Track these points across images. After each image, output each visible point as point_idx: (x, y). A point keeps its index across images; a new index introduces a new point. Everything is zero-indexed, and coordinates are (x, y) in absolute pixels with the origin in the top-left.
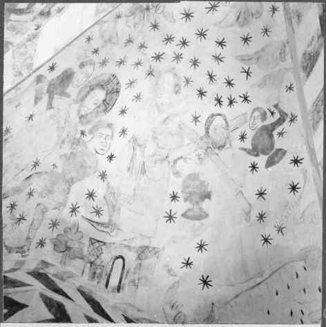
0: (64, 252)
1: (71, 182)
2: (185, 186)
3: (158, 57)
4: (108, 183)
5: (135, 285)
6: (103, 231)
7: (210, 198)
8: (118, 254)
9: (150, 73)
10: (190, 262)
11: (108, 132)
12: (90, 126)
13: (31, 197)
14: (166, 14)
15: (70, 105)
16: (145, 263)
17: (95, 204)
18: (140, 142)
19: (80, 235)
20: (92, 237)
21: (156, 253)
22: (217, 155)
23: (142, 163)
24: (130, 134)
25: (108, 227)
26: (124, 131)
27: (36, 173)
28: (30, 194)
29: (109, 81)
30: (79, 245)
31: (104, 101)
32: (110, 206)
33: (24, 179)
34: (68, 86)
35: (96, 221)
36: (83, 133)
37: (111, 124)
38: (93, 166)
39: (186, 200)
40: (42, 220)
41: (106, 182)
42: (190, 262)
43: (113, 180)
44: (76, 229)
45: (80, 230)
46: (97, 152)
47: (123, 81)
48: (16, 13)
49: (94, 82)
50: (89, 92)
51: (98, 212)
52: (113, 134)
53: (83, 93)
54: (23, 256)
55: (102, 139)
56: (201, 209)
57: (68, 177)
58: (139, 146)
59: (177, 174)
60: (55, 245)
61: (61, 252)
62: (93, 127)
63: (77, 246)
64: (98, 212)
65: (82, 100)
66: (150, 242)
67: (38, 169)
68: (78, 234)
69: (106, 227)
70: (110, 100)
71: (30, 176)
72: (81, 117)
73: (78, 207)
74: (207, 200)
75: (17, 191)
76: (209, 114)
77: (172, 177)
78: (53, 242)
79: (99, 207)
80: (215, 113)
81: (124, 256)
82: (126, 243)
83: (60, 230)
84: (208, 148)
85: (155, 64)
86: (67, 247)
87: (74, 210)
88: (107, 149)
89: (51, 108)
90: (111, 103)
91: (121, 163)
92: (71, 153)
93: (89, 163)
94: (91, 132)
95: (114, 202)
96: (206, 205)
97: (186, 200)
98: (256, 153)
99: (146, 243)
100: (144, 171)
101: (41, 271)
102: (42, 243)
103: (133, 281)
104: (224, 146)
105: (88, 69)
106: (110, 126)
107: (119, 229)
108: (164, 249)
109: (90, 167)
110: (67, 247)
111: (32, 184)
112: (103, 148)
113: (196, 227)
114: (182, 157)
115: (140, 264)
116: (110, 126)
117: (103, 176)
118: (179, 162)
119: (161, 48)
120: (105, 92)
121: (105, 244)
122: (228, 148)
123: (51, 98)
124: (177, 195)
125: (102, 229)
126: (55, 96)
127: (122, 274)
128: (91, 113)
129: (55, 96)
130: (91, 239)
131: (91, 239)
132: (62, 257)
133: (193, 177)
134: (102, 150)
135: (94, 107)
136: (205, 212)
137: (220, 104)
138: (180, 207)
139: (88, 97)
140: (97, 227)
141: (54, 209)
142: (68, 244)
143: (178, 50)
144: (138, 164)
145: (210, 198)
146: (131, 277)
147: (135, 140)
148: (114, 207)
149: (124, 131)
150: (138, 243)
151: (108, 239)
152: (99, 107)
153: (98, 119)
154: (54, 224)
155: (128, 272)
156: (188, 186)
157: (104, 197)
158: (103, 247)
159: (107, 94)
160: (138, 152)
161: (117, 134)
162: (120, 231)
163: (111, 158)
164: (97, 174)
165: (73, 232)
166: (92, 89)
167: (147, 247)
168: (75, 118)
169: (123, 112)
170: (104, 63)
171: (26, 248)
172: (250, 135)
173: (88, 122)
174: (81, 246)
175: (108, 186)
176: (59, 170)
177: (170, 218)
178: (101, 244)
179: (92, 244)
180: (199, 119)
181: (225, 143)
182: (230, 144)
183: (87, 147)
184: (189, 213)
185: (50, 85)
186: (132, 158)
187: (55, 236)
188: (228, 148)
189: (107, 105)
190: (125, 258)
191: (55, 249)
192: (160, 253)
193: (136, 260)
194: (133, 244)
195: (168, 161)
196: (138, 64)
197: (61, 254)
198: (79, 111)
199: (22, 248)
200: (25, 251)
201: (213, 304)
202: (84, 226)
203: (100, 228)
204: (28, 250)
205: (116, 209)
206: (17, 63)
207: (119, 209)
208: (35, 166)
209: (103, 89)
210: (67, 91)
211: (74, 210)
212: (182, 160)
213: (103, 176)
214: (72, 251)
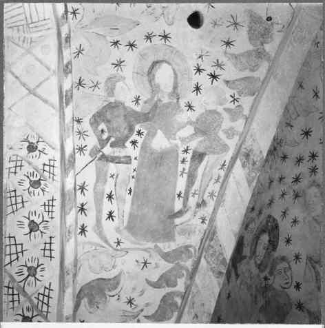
3: (297, 180)
4: (308, 310)
9: (297, 196)
11: (284, 265)
12: (268, 270)
14: (289, 142)
24: (304, 257)
31: (270, 241)
41: (305, 310)
47: (277, 215)
48: (178, 217)
52: (288, 264)
58: (316, 263)
85: (296, 187)
94: (271, 273)
116: (283, 259)
119: (297, 171)
134: (287, 283)
135: (264, 251)
143: (310, 165)
147: (310, 259)
149: (297, 257)
159: (269, 235)
160: (317, 266)
163: (298, 286)
168: (255, 271)
170: (260, 213)
173: (266, 267)
183: (274, 289)
186: (316, 277)
189: (273, 244)
196: (283, 194)
198: (256, 262)
206: (214, 265)
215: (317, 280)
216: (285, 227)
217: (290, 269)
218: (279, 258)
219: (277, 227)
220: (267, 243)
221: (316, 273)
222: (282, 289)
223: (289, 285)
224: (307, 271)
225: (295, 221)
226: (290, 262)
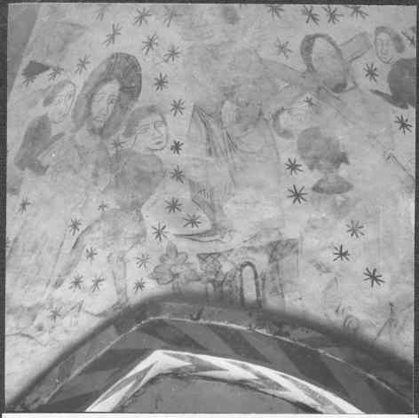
2: (303, 149)
4: (190, 181)
5: (278, 294)
7: (347, 162)
8: (242, 262)
10: (343, 251)
13: (95, 256)
16: (284, 262)
17: (183, 214)
21: (293, 246)
22: (338, 99)
25: (216, 234)
27: (83, 232)
31: (122, 89)
35: (195, 232)
37: (153, 106)
39: (311, 168)
42: (343, 251)
43: (195, 174)
56: (337, 177)
59: (286, 134)
60: (157, 279)
61: (169, 282)
62: (129, 126)
64: (193, 222)
66: (280, 234)
67: (82, 228)
68: (180, 257)
69: (213, 235)
71: (78, 239)
74: (343, 165)
76: (300, 37)
77: (280, 140)
78: (153, 278)
80: (312, 32)
81: (251, 261)
82: (247, 245)
84: (319, 88)
96: (343, 171)
97: (311, 168)
98: (401, 104)
99: (274, 237)
100: (233, 146)
103: (275, 289)
104: (344, 85)
106: (152, 110)
107: (230, 231)
108: (302, 239)
111: (85, 246)
112: (158, 140)
113: (339, 204)
114: (283, 109)
115: (277, 267)
116: (152, 110)
117: (178, 175)
118: (283, 118)
120: (115, 81)
121: (220, 254)
122: (352, 89)
124: (297, 163)
125: (213, 238)
126: (39, 158)
127: (257, 285)
128: (113, 113)
129: (39, 158)
130: (199, 256)
133: (311, 135)
135: (111, 106)
136: (347, 183)
137: (314, 19)
138: (307, 178)
144: (220, 142)
145: (347, 162)
146: (269, 285)
150: (264, 241)
151: (221, 248)
155: (264, 280)
156: (308, 148)
158: (219, 259)
160: (211, 120)
162: (232, 233)
167: (279, 242)
168: (92, 143)
169: (161, 83)
172: (384, 71)
173: (118, 125)
174: (191, 267)
175: (192, 184)
177: (297, 195)
178: (215, 256)
179: (204, 260)
180: (288, 47)
181: (345, 80)
182: (354, 83)
183: (135, 153)
184: (322, 186)
186: (208, 135)
188: (352, 89)
189: (131, 89)
190: (255, 263)
191: (159, 283)
192: (299, 246)
193: (270, 262)
194: (257, 244)
195: (265, 120)
198: (93, 131)
201: (391, 304)
202: (183, 245)
203: (207, 239)
205: (217, 208)
207: (221, 208)
209: (111, 80)
211: (159, 233)
212: (286, 113)
213: (178, 175)
216: (150, 66)
217: (166, 124)
219: (135, 66)
222: (149, 153)
225: (173, 53)
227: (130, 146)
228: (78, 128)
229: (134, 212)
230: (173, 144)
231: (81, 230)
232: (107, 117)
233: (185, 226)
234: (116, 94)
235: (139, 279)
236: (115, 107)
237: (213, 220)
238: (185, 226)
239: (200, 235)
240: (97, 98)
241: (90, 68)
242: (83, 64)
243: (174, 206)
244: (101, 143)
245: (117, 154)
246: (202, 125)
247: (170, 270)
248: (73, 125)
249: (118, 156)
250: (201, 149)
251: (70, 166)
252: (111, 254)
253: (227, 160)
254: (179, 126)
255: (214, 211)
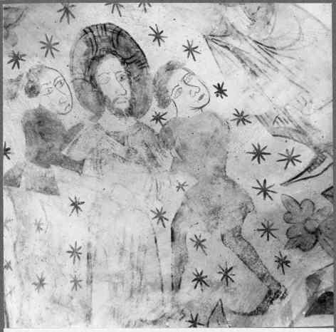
0: (317, 241)
1: (221, 171)
6: (326, 169)
11: (178, 74)
15: (97, 126)
18: (219, 30)
19: (307, 203)
20: (323, 190)
23: (256, 46)
24: (199, 41)
26: (190, 50)
27: (174, 220)
28: (199, 243)
29: (92, 44)
30: (322, 215)
31: (124, 61)
32: (294, 135)
33: (170, 243)
34: (60, 124)
36: (158, 118)
38: (218, 124)
40: (249, 244)
43: (257, 106)
44: (294, 204)
45: (300, 201)
46: (201, 108)
49: (80, 71)
50: (95, 86)
51: (291, 159)
53: (91, 98)
54: (283, 298)
55: (186, 89)
57: (210, 171)
60: (298, 246)
61: (314, 244)
62: (159, 96)
63: (321, 219)
64: (291, 159)
65: (102, 100)
69: (322, 162)
70: (128, 50)
72: (130, 112)
73: (265, 181)
75: (181, 262)
79: (284, 152)
83: (281, 226)
86: (313, 233)
87: (265, 191)
88: (203, 91)
89: (82, 163)
90: (134, 51)
91: (236, 79)
92: (177, 151)
93: (208, 130)
94: (164, 103)
95: (290, 125)
100: (270, 50)
101: (319, 295)
102: (283, 263)
105: (44, 82)
106: (170, 68)
109: (216, 131)
110: (313, 233)
112: (198, 96)
116: (170, 68)
117: (241, 118)
120: (109, 55)
123: (65, 162)
128: (133, 90)
131: (323, 194)
132: (323, 248)
134: (201, 98)
139: (104, 88)
140: (313, 173)
141: (244, 218)
142: (310, 227)
144: (255, 56)
147: (211, 38)
148: (299, 130)
149: (190, 50)
152: (129, 75)
153: (150, 83)
154: (267, 230)
157: (274, 136)
159: (115, 54)
160: (230, 40)
161: (190, 64)
163: (220, 90)
164: (232, 124)
165: (296, 208)
166: (92, 78)
168: (125, 125)
169: (158, 36)
170: (49, 47)
171: (274, 288)
173: (146, 100)
176: (191, 182)
185: (38, 159)
186: (238, 57)
187: (284, 239)
189: (134, 60)
191: (304, 250)
197: (318, 247)
198: (119, 113)
199: (270, 292)
200: (278, 291)
202: (299, 191)
204: (279, 285)
207: (307, 124)
208: (161, 219)
209: (102, 56)
210: (68, 126)
211: (265, 191)
213: (241, 118)
214: (323, 229)
215: (242, 61)
217: (193, 74)
218: (164, 70)
219: (119, 33)
220: (122, 68)
221: (233, 52)
223: (206, 97)
224: (220, 58)
226: (184, 64)
227: (174, 116)
228: (98, 114)
229: (221, 180)
230: (216, 90)
231: (171, 220)
232: (129, 95)
233: (286, 168)
234: (123, 70)
235: (278, 255)
236: (130, 83)
237: (309, 144)
238: (286, 168)
239: (308, 169)
240: (100, 80)
241: (65, 48)
242: (49, 47)
243: (259, 154)
244: (138, 123)
245: (163, 129)
246: (225, 51)
247: (305, 228)
248: (89, 114)
249: (166, 130)
250: (241, 74)
251: (114, 155)
252: (223, 237)
253: (276, 69)
254: (208, 68)
255: (304, 134)
